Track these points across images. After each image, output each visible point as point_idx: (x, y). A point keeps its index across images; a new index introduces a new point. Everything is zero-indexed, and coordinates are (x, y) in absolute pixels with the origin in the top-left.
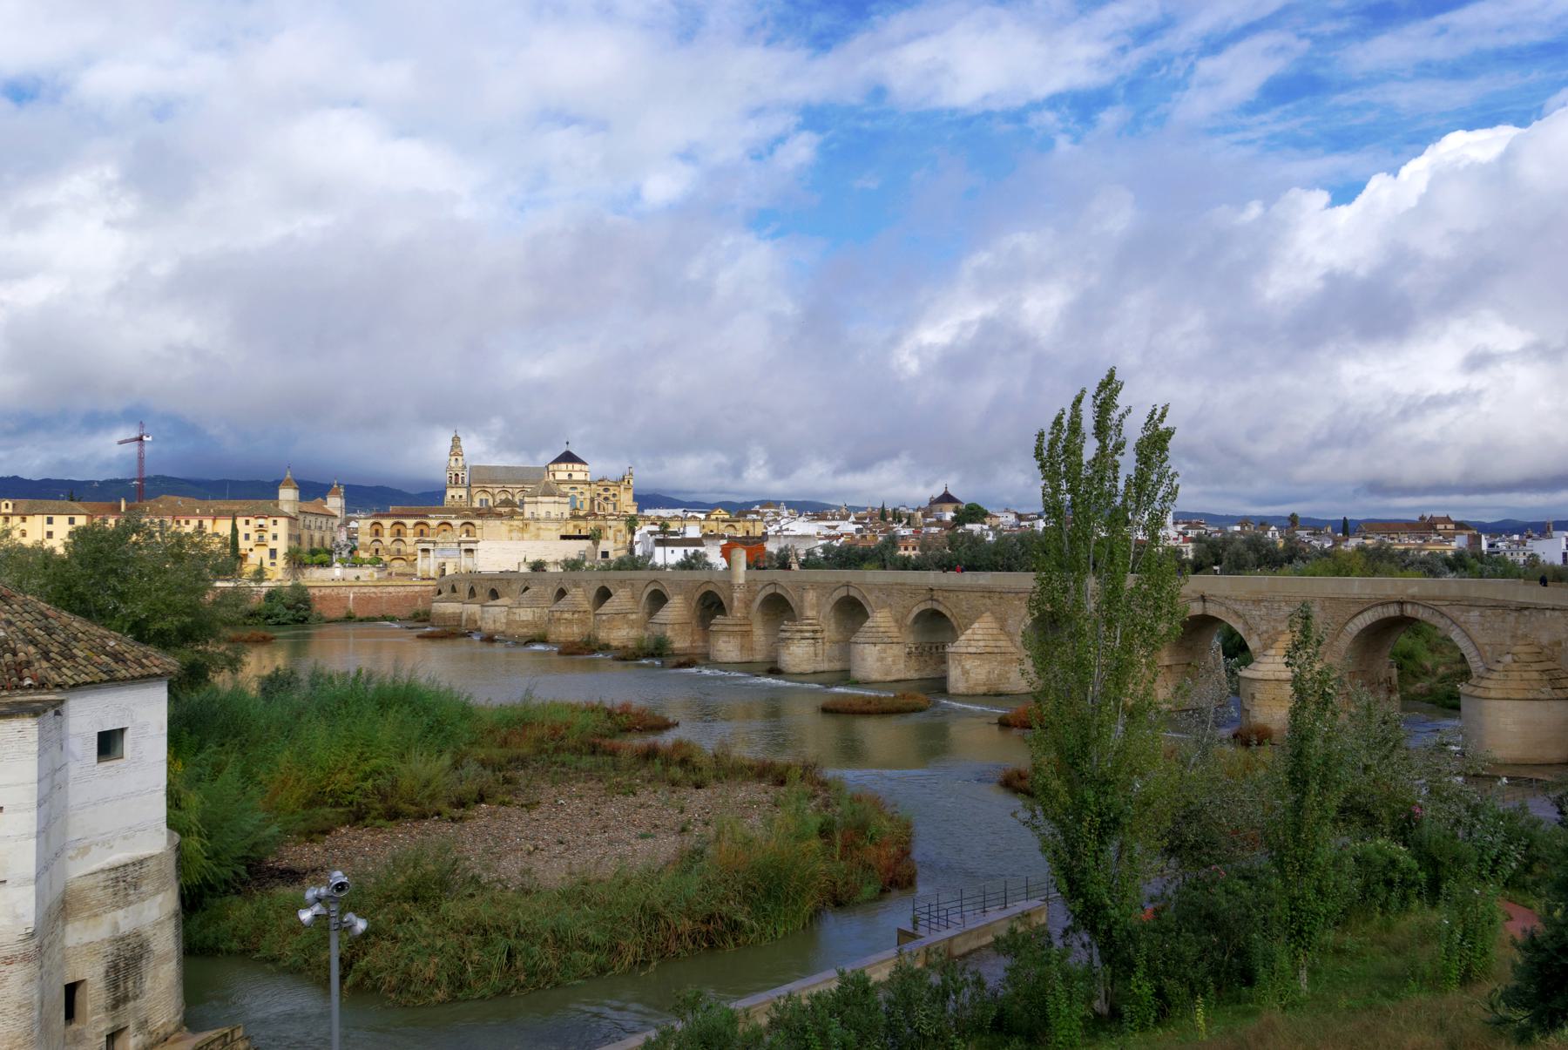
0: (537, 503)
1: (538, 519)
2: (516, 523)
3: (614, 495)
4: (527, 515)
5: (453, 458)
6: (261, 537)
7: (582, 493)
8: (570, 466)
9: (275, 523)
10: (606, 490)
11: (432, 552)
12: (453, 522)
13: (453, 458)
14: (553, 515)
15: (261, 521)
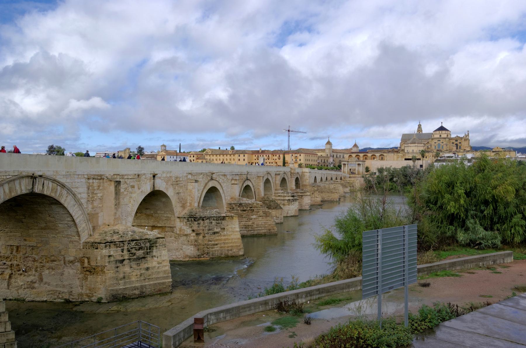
0: (408, 146)
1: (409, 153)
2: (400, 154)
3: (460, 143)
4: (406, 151)
5: (418, 132)
6: (296, 160)
7: (442, 142)
8: (441, 132)
9: (300, 155)
10: (456, 141)
11: (347, 165)
12: (376, 155)
13: (418, 132)
14: (415, 151)
15: (296, 155)
